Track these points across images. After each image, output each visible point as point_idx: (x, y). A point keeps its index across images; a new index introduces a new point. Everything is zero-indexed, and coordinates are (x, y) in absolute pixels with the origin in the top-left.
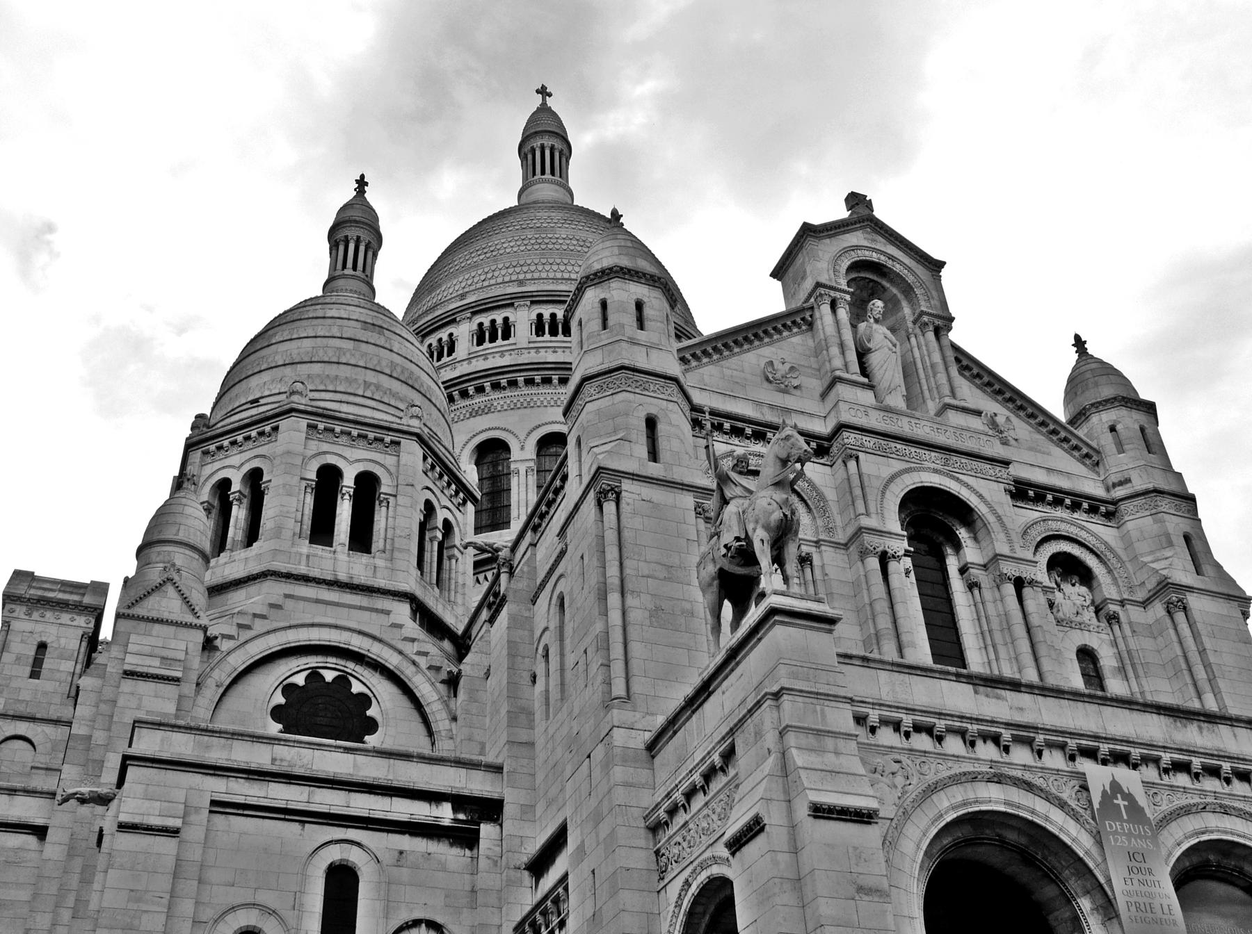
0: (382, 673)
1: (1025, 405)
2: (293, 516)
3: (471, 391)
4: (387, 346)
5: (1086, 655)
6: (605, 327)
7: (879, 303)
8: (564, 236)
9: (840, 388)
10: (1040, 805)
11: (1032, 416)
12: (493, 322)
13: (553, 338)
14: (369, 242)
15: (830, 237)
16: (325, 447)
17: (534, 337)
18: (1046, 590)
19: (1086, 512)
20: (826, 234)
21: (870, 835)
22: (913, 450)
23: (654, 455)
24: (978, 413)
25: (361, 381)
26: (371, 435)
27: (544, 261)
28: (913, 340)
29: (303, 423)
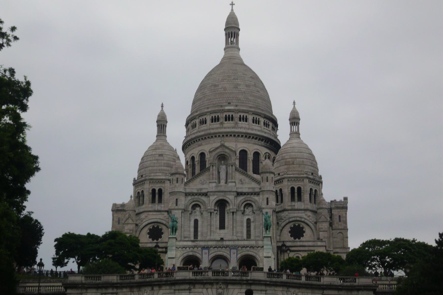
4: (163, 159)
5: (248, 220)
7: (223, 162)
8: (220, 88)
9: (210, 184)
10: (196, 254)
11: (249, 177)
12: (203, 119)
13: (215, 123)
16: (153, 185)
18: (241, 211)
21: (174, 260)
23: (177, 205)
24: (235, 182)
26: (160, 181)
27: (215, 98)
28: (228, 168)
29: (148, 182)
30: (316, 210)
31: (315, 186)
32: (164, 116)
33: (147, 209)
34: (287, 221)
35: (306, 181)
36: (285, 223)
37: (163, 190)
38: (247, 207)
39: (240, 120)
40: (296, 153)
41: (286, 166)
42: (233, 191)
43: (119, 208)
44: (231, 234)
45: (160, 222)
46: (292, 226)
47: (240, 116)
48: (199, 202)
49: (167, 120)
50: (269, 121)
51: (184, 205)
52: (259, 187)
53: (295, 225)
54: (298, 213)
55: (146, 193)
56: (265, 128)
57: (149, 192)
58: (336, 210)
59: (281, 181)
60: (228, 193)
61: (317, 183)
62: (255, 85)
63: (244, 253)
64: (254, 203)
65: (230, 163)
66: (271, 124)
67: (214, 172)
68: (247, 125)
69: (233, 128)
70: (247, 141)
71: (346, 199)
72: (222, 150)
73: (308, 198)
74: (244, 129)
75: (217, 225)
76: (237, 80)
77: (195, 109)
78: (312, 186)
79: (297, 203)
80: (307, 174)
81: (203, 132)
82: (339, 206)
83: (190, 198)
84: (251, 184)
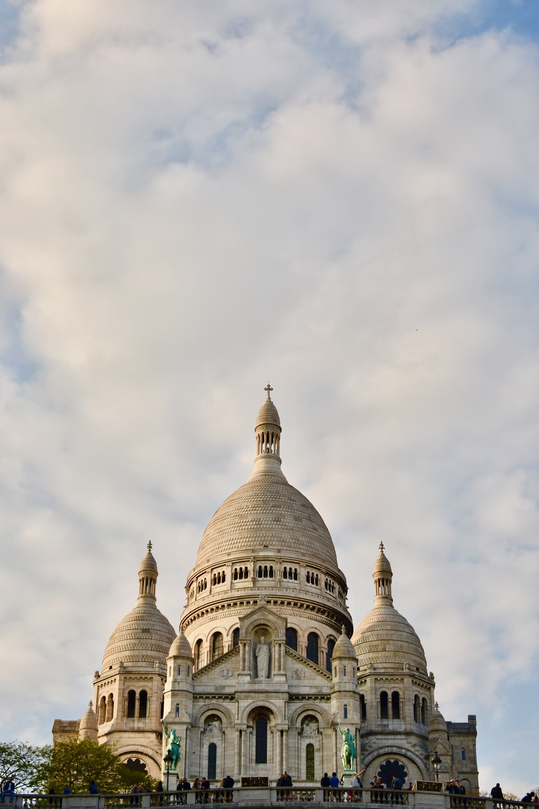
0: (148, 757)
1: (309, 663)
2: (121, 711)
3: (209, 610)
4: (150, 638)
5: (310, 747)
6: (170, 676)
7: (262, 638)
8: (250, 520)
9: (239, 677)
12: (219, 573)
13: (241, 580)
14: (151, 578)
15: (247, 619)
16: (130, 684)
17: (234, 580)
19: (320, 700)
20: (246, 618)
22: (257, 695)
24: (285, 675)
25: (141, 656)
26: (144, 677)
27: (240, 537)
28: (273, 648)
29: (123, 677)
30: (427, 735)
31: (422, 691)
32: (153, 563)
33: (118, 728)
34: (375, 754)
35: (408, 681)
36: (370, 757)
37: (149, 692)
39: (285, 577)
40: (388, 632)
41: (371, 655)
42: (281, 691)
43: (67, 729)
45: (142, 751)
46: (384, 763)
47: (285, 568)
48: (219, 710)
49: (156, 569)
50: (333, 581)
51: (191, 716)
52: (330, 685)
53: (390, 761)
54: (395, 739)
55: (116, 699)
56: (328, 592)
57: (123, 697)
58: (456, 738)
59: (363, 681)
60: (273, 694)
61: (426, 686)
62: (309, 519)
64: (321, 715)
65: (277, 640)
66: (337, 586)
67: (247, 656)
68: (296, 584)
69: (272, 589)
70: (297, 612)
71: (472, 718)
72: (262, 617)
73: (412, 712)
74: (293, 591)
75: (252, 755)
76: (280, 507)
77: (205, 558)
78: (418, 692)
79: (393, 721)
80: (409, 669)
81: (219, 595)
82: (460, 731)
83: (201, 703)
84: (315, 679)
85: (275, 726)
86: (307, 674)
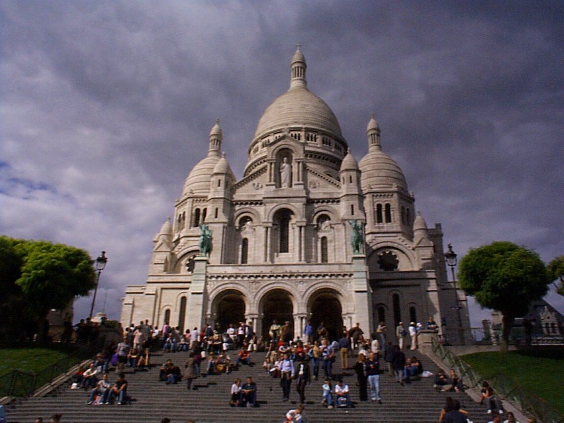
7: (285, 158)
10: (239, 287)
16: (196, 204)
21: (201, 296)
23: (216, 217)
38: (321, 220)
39: (308, 140)
44: (298, 259)
47: (309, 135)
54: (390, 237)
55: (186, 214)
60: (294, 199)
63: (319, 286)
66: (343, 149)
71: (438, 226)
84: (327, 187)
85: (295, 224)
86: (321, 184)
